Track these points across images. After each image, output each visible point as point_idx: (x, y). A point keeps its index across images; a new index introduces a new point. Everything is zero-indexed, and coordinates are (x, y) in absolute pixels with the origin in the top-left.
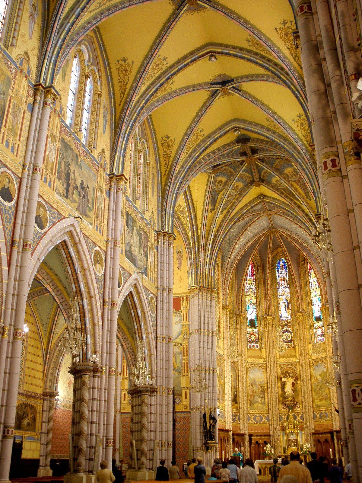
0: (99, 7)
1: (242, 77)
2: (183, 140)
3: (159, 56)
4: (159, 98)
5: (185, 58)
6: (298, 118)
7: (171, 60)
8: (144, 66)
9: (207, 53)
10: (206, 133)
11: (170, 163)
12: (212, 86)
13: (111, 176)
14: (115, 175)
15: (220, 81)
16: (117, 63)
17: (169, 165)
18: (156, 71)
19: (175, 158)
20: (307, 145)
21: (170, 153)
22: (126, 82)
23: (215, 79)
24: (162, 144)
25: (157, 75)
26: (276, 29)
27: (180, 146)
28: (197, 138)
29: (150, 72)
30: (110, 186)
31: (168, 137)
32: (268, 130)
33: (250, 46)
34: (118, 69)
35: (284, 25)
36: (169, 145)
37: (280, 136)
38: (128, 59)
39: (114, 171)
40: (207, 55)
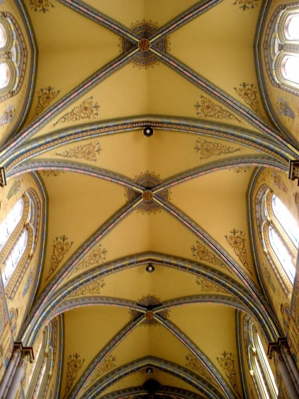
0: (66, 156)
1: (172, 301)
2: (93, 362)
3: (100, 245)
4: (85, 297)
5: (123, 259)
6: (223, 357)
7: (110, 257)
8: (82, 248)
9: (146, 260)
10: (118, 363)
11: (73, 386)
12: (138, 307)
13: (16, 345)
14: (22, 346)
15: (146, 305)
16: (55, 240)
17: (72, 388)
18: (92, 262)
19: (79, 381)
20: (232, 387)
21: (75, 375)
22: (59, 260)
23: (142, 300)
24: (69, 364)
25: (91, 267)
26: (226, 237)
27: (88, 369)
28: (107, 366)
29: (87, 259)
30: (12, 356)
31: (77, 357)
32: (186, 370)
33: (194, 255)
34: (55, 246)
35: (234, 234)
36: (76, 366)
37: (198, 378)
38: (67, 238)
39: (23, 340)
40: (146, 263)
